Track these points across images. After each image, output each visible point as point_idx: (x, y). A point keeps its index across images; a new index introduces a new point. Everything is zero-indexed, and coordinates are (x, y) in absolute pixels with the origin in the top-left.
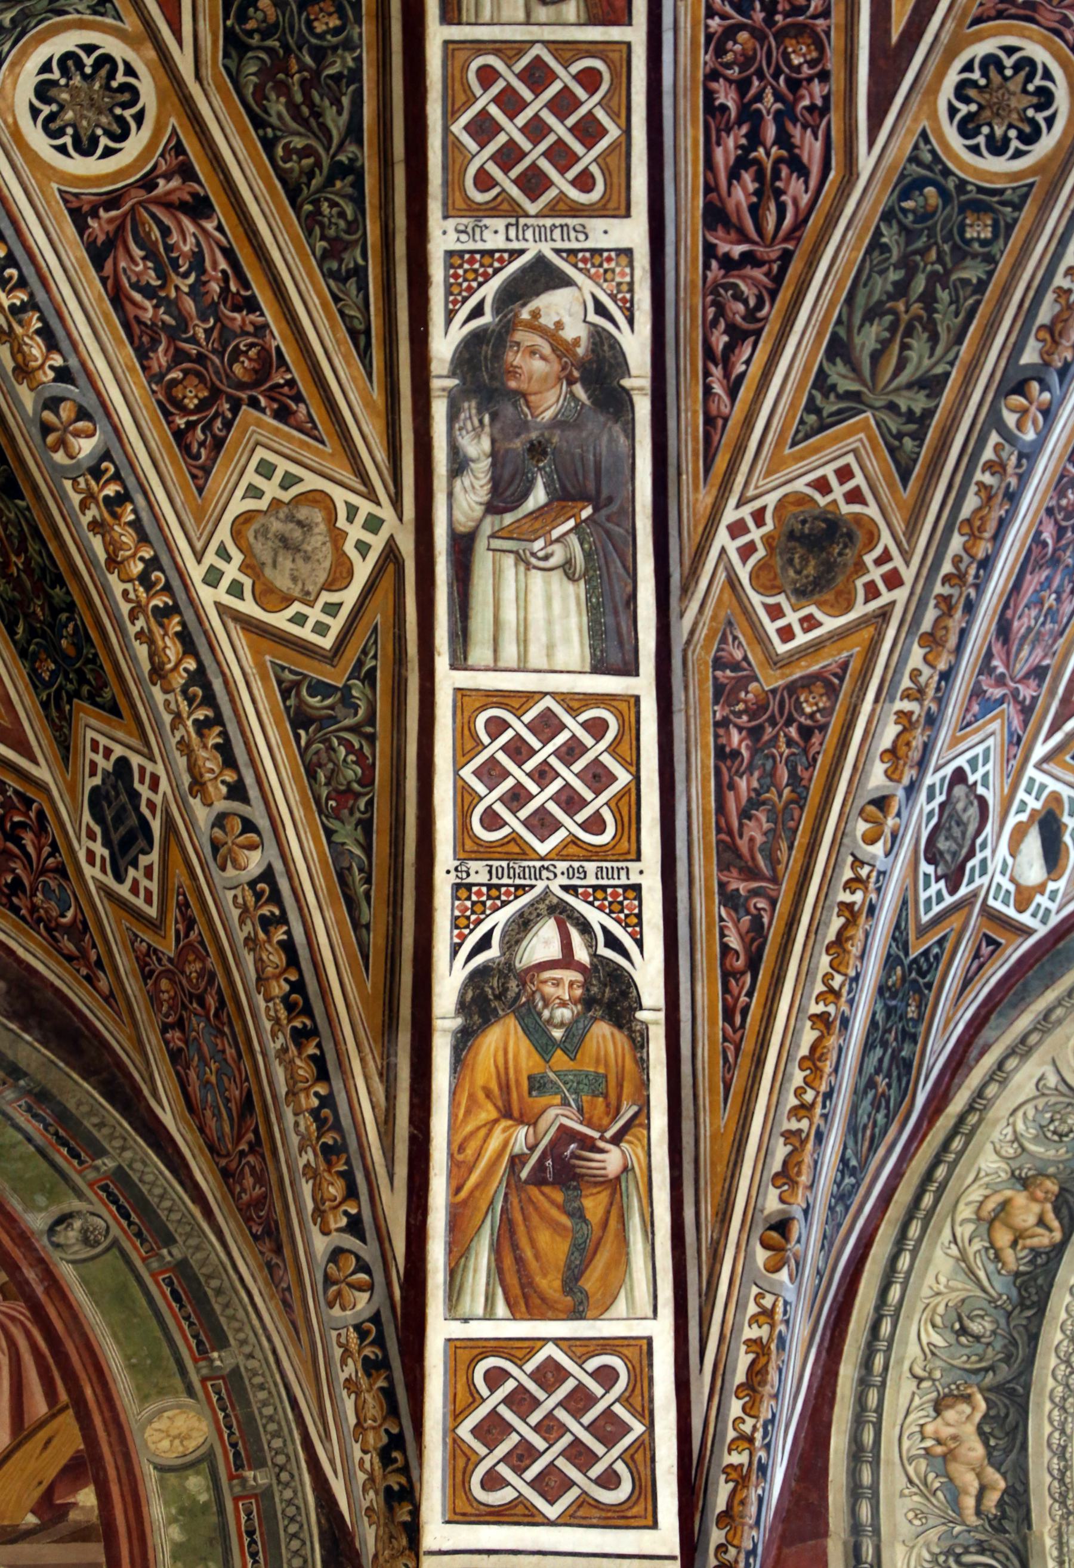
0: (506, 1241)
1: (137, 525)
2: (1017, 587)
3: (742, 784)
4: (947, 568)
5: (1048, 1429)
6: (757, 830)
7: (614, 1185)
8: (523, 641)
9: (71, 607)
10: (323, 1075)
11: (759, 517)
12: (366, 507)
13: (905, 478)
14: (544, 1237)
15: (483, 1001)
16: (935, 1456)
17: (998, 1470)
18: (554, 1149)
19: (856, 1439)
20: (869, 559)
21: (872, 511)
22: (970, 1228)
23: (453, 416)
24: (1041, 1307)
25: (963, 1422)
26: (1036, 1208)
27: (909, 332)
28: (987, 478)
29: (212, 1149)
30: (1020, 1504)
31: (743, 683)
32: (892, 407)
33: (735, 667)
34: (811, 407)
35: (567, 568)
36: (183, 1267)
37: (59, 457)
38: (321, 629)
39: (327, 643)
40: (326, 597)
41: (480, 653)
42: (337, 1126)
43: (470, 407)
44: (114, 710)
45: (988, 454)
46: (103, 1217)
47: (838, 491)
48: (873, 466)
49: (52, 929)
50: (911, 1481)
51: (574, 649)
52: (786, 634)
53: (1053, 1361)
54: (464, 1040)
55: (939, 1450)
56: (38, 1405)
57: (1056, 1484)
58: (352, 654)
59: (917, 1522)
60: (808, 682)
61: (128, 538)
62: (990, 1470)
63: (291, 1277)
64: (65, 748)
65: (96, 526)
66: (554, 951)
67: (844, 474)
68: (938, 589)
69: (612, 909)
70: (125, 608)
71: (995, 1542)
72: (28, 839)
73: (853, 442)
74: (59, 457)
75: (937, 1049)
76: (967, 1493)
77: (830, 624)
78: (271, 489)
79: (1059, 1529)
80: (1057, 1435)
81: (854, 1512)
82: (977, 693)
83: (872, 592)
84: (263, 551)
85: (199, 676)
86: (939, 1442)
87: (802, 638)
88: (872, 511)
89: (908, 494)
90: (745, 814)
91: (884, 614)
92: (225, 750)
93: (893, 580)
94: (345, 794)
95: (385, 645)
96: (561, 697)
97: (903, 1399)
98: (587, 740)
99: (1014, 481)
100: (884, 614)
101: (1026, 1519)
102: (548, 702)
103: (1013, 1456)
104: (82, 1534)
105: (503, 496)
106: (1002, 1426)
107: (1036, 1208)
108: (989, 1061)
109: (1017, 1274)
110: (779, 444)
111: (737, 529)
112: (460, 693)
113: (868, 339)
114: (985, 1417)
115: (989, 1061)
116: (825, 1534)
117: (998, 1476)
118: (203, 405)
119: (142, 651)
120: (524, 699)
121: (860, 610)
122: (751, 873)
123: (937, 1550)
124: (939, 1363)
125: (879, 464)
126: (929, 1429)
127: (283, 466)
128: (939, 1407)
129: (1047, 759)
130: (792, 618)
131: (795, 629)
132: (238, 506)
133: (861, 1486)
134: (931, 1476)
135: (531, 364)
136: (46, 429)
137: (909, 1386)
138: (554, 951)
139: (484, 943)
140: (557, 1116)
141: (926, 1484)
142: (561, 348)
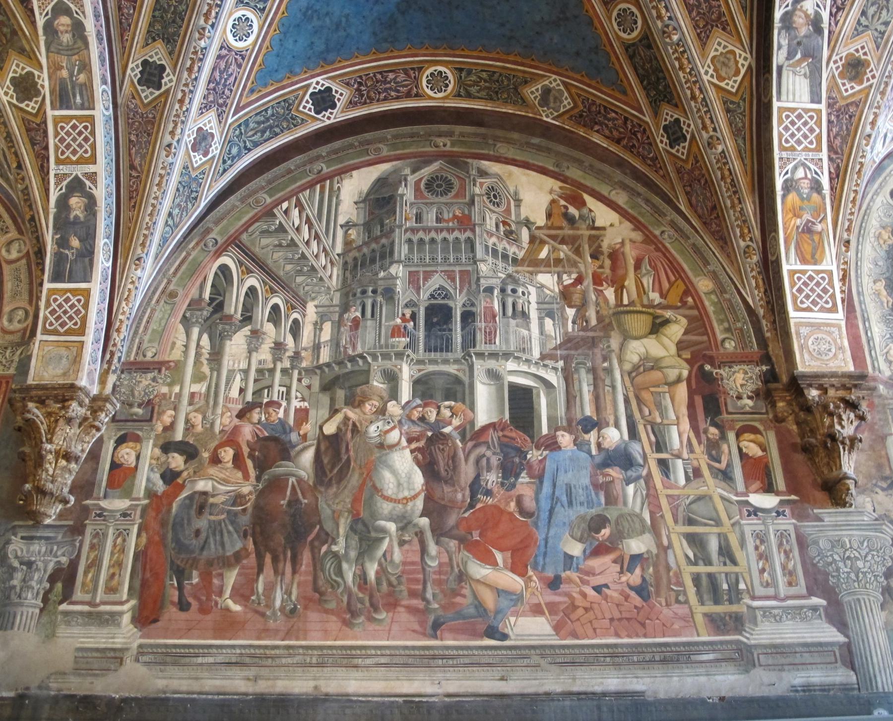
0: (798, 248)
1: (688, 59)
6: (838, 142)
7: (820, 233)
8: (794, 95)
9: (665, 78)
10: (740, 203)
11: (841, 59)
12: (744, 54)
14: (806, 246)
15: (789, 186)
18: (806, 224)
23: (779, 34)
29: (700, 217)
35: (805, 75)
37: (668, 40)
38: (733, 87)
39: (734, 90)
41: (784, 97)
43: (783, 32)
44: (676, 106)
46: (672, 232)
49: (644, 158)
51: (806, 97)
52: (846, 90)
54: (784, 197)
56: (673, 278)
58: (740, 93)
60: (851, 104)
61: (686, 62)
63: (730, 250)
64: (656, 114)
65: (676, 59)
66: (803, 175)
69: (816, 164)
70: (683, 81)
72: (639, 136)
74: (668, 40)
77: (857, 88)
78: (721, 49)
83: (868, 80)
84: (719, 66)
85: (704, 99)
87: (850, 92)
90: (835, 138)
91: (871, 86)
92: (711, 118)
93: (873, 77)
94: (739, 130)
95: (748, 90)
96: (803, 109)
100: (871, 86)
105: (790, 55)
111: (835, 62)
112: (779, 108)
118: (704, 26)
119: (688, 92)
121: (865, 84)
122: (836, 153)
127: (724, 43)
128: (875, 282)
130: (848, 86)
131: (849, 89)
132: (712, 54)
135: (799, 20)
136: (664, 32)
138: (803, 175)
139: (787, 173)
140: (807, 216)
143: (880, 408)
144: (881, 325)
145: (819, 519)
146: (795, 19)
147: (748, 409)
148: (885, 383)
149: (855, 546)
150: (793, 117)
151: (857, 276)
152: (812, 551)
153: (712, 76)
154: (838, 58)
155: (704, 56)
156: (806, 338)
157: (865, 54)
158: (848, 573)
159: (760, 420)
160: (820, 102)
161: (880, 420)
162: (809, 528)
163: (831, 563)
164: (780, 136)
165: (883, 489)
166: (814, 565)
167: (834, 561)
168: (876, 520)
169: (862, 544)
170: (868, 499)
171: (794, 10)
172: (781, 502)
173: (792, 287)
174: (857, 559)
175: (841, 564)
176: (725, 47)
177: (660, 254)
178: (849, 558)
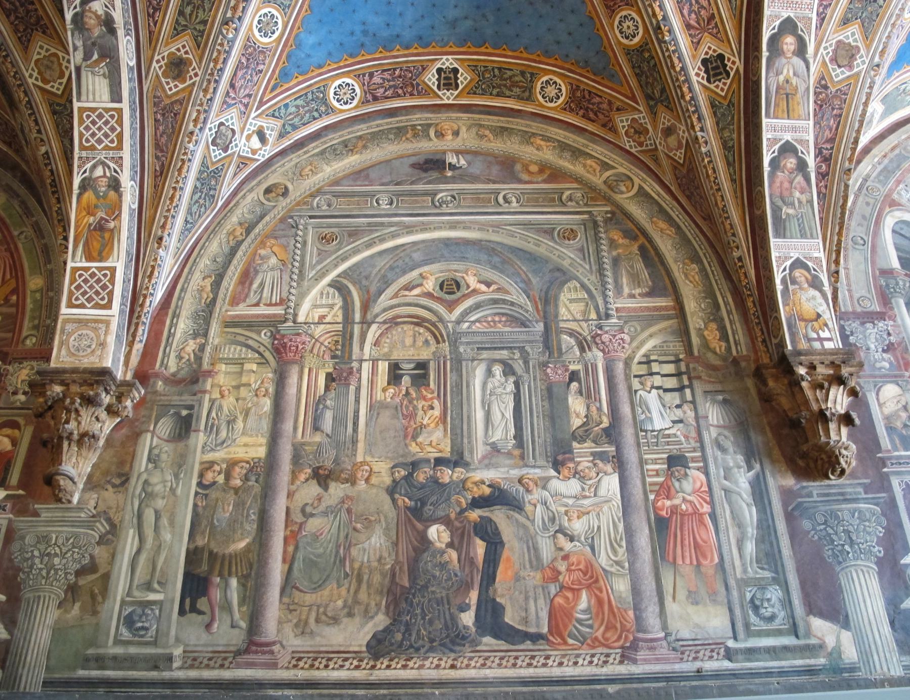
2: (235, 74)
3: (161, 128)
4: (209, 71)
6: (164, 140)
7: (112, 231)
8: (94, 94)
11: (163, 58)
13: (199, 47)
15: (83, 187)
18: (99, 222)
19: (183, 286)
20: (190, 69)
21: (191, 56)
23: (73, 35)
25: (208, 282)
27: (198, 8)
28: (219, 48)
31: (160, 102)
32: (195, 29)
33: (158, 98)
34: (175, 29)
35: (104, 75)
36: (45, 245)
38: (58, 89)
39: (60, 93)
40: (59, 81)
41: (84, 98)
42: (62, 215)
43: (76, 33)
45: (219, 41)
47: (183, 51)
48: (191, 44)
51: (106, 96)
52: (170, 89)
54: (80, 195)
60: (176, 102)
66: (101, 174)
67: (184, 47)
68: (207, 77)
69: (116, 163)
73: (186, 38)
75: (226, 191)
77: (181, 86)
82: (225, 102)
83: (191, 78)
84: (42, 69)
85: (29, 102)
87: (174, 90)
88: (191, 56)
89: (199, 52)
90: (161, 136)
91: (194, 84)
92: (36, 121)
93: (196, 75)
96: (104, 109)
97: (197, 276)
98: (110, 120)
99: (227, 49)
100: (194, 84)
102: (100, 110)
104: (12, 306)
105: (87, 56)
110: (167, 39)
111: (158, 61)
113: (188, 10)
120: (93, 110)
121: (188, 82)
122: (162, 151)
125: (192, 43)
128: (204, 279)
129: (257, 117)
130: (172, 85)
131: (172, 87)
132: (36, 57)
135: (91, 22)
137: (199, 273)
138: (101, 174)
139: (85, 172)
140: (101, 214)
142: (98, 17)
143: (148, 405)
144: (189, 322)
145: (36, 514)
146: (86, 20)
147: (18, 404)
148: (167, 381)
149: (60, 541)
150: (94, 117)
152: (15, 546)
153: (37, 79)
154: (160, 57)
155: (27, 60)
156: (69, 335)
157: (186, 53)
158: (41, 569)
159: (25, 416)
160: (120, 101)
161: (143, 416)
162: (22, 522)
163: (28, 559)
164: (81, 135)
165: (114, 486)
166: (11, 560)
167: (33, 556)
168: (93, 516)
169: (68, 540)
170: (96, 496)
171: (83, 11)
172: (7, 497)
173: (71, 284)
174: (56, 555)
175: (37, 561)
176: (47, 50)
177: (8, 254)
178: (49, 555)
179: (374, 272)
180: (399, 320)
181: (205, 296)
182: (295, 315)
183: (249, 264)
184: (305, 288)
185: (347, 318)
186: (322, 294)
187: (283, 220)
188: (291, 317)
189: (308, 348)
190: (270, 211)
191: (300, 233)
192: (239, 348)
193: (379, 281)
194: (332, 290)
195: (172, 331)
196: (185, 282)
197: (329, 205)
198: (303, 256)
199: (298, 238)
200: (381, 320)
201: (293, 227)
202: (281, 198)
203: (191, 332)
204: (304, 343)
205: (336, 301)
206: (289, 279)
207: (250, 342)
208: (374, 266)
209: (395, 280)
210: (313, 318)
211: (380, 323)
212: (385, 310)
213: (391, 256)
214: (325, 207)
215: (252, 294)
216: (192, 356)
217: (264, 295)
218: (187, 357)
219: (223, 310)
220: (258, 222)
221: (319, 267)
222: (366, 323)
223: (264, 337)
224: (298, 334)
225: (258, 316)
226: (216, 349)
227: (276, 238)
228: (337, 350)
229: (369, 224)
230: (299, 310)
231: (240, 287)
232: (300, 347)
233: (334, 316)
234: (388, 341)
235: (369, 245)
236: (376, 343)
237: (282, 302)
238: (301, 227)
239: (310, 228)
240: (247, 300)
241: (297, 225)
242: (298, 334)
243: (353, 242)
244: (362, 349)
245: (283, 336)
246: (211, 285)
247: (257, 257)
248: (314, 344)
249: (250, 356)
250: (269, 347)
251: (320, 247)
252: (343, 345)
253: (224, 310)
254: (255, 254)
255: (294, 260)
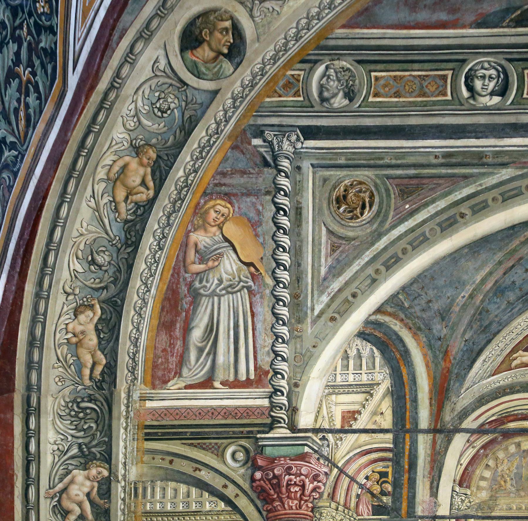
5: (131, 327)
16: (71, 344)
17: (103, 353)
22: (103, 185)
24: (136, 245)
25: (88, 321)
26: (141, 171)
30: (112, 374)
50: (59, 359)
53: (139, 283)
55: (74, 340)
57: (131, 361)
59: (60, 384)
62: (99, 353)
71: (97, 395)
76: (86, 367)
79: (129, 388)
80: (134, 331)
81: (28, 378)
86: (75, 335)
101: (114, 383)
103: (111, 344)
106: (108, 325)
107: (141, 171)
108: (125, 44)
109: (126, 222)
114: (100, 319)
115: (125, 44)
116: (13, 390)
117: (102, 356)
123: (68, 400)
124: (79, 283)
126: (70, 327)
128: (76, 313)
133: (33, 363)
134: (69, 356)
137: (62, 298)
141: (66, 361)
144: (63, 426)
151: (38, 296)
179: (460, 301)
180: (512, 425)
181: (88, 360)
182: (293, 411)
183: (176, 272)
184: (308, 344)
185: (403, 419)
186: (346, 357)
187: (239, 141)
188: (282, 414)
189: (327, 490)
190: (205, 107)
191: (284, 182)
192: (183, 488)
193: (470, 325)
194: (367, 349)
195: (33, 447)
196: (34, 321)
197: (350, 95)
198: (297, 252)
199: (282, 200)
200: (474, 426)
201: (266, 164)
202: (227, 66)
203: (75, 451)
204: (316, 478)
205: (378, 377)
206: (270, 319)
207: (204, 475)
208: (460, 284)
209: (508, 323)
210: (331, 419)
211: (472, 432)
212: (482, 401)
213: (499, 256)
214: (339, 101)
215: (193, 355)
216: (87, 506)
217: (221, 359)
218: (77, 511)
219: (136, 396)
220: (180, 146)
221: (336, 285)
222: (443, 432)
223: (231, 461)
224: (303, 457)
225: (213, 411)
226: (135, 490)
227: (228, 197)
228: (383, 493)
229: (450, 159)
230: (299, 396)
231: (164, 337)
232: (310, 487)
233: (374, 413)
234: (487, 474)
235: (448, 224)
236: (464, 480)
237: (261, 378)
238: (285, 164)
239: (306, 165)
240: (185, 371)
241: (275, 158)
242: (303, 457)
243: (412, 213)
244: (434, 492)
245: (272, 460)
246: (97, 331)
247: (191, 255)
248: (337, 479)
249: (208, 507)
250: (246, 486)
251: (335, 228)
252: (396, 485)
253: (138, 398)
254: (185, 245)
255: (279, 264)
